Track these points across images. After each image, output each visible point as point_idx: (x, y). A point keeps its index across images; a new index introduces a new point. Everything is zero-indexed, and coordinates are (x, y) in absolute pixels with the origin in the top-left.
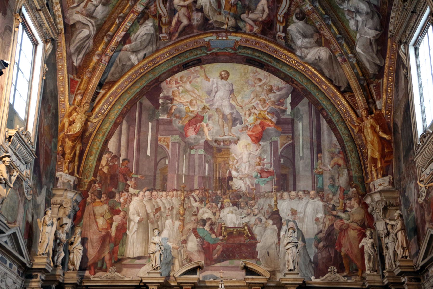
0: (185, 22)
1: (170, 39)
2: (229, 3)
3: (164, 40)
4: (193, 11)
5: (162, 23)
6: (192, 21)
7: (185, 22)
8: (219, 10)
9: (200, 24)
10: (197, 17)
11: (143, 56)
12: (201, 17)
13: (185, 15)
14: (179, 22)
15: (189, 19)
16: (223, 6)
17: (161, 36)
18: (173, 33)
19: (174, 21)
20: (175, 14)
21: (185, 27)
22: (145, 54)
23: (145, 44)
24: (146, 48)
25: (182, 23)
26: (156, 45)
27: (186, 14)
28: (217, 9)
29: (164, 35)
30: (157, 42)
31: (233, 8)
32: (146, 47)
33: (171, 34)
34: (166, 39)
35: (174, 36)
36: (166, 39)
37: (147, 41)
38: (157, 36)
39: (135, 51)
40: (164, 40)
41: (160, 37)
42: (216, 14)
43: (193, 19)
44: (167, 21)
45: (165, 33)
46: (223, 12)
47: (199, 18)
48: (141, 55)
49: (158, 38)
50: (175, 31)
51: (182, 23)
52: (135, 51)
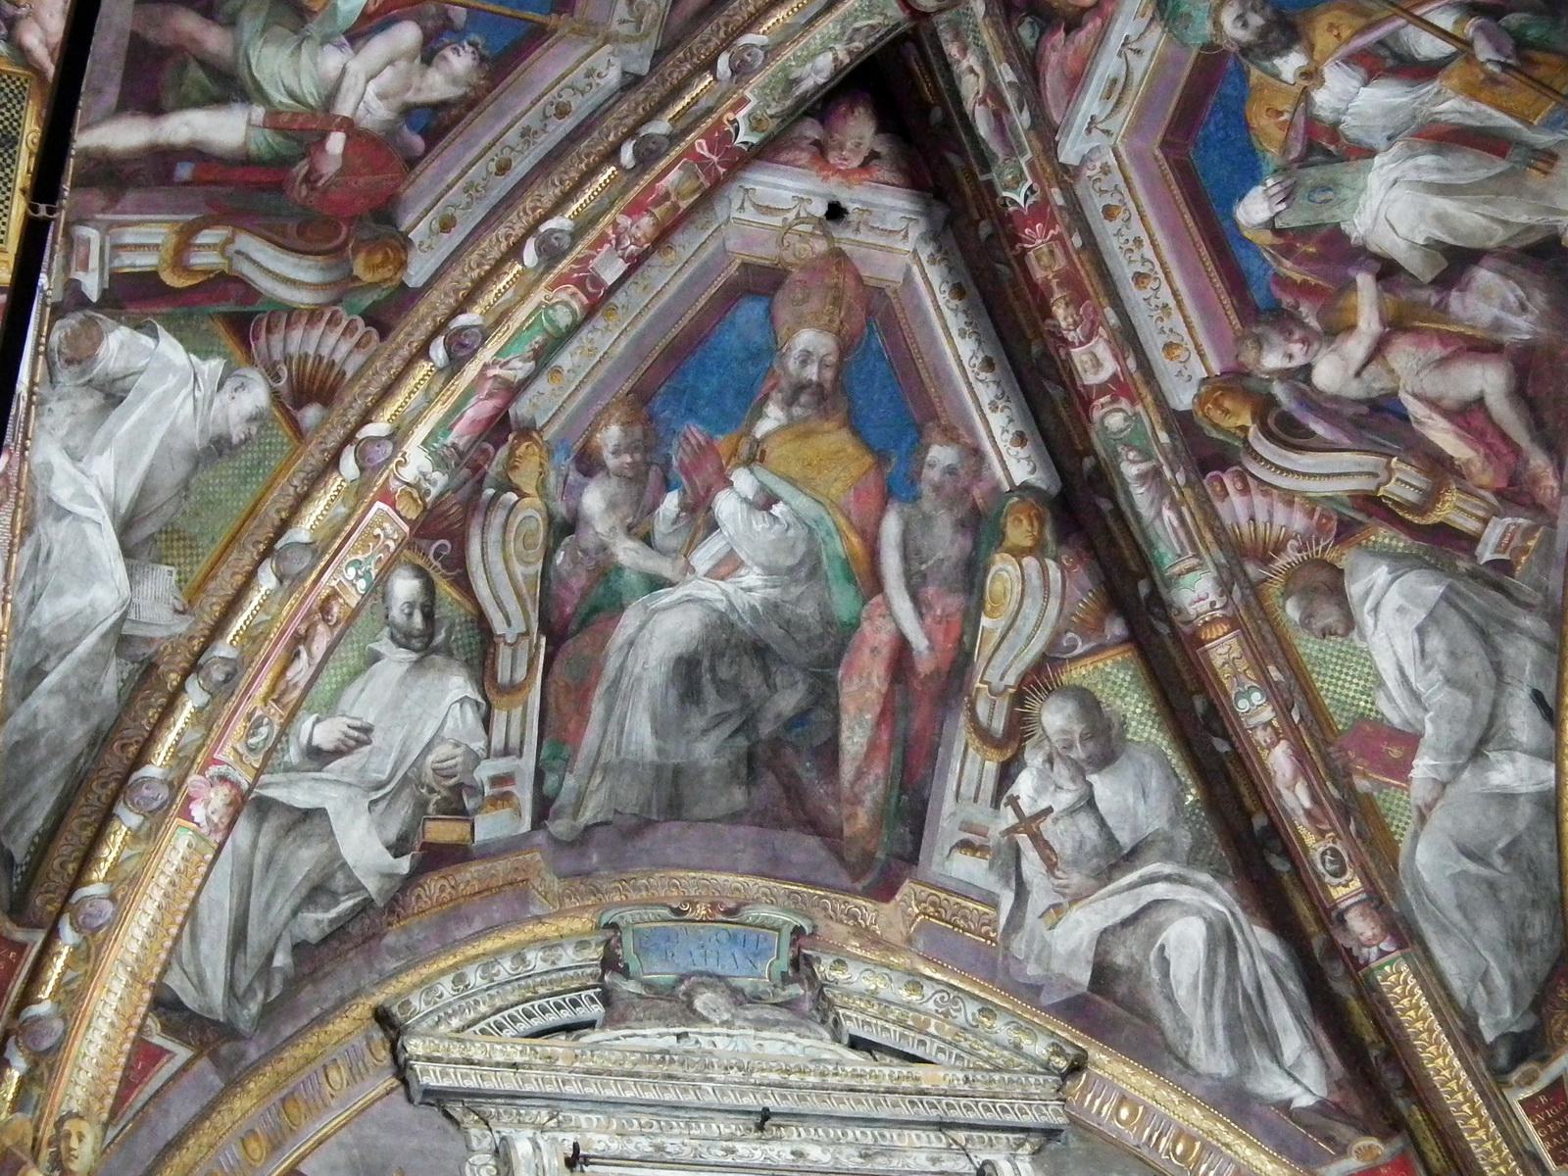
0: (1488, 380)
1: (1540, 510)
2: (1492, 80)
3: (1525, 551)
4: (1442, 308)
5: (1413, 508)
6: (1507, 338)
7: (1488, 380)
8: (1515, 155)
9: (1550, 303)
10: (1491, 300)
11: (1538, 716)
12: (1505, 275)
13: (1442, 363)
14: (1468, 415)
15: (1480, 347)
16: (1501, 120)
17: (1486, 553)
18: (1513, 480)
19: (1443, 436)
20: (1404, 417)
21: (1522, 392)
22: (1538, 697)
23: (1475, 665)
24: (1509, 671)
25: (1480, 401)
26: (1528, 607)
27: (1437, 351)
28: (1501, 166)
29: (1493, 533)
30: (1509, 595)
31: (1540, 72)
32: (1498, 669)
33: (1515, 494)
34: (1528, 533)
35: (1535, 481)
36: (1528, 533)
37: (1470, 643)
38: (1474, 575)
39: (1483, 741)
40: (1525, 551)
41: (1491, 563)
42: (1535, 180)
43: (1498, 325)
44: (1419, 481)
45: (1485, 522)
46: (1544, 139)
47: (1511, 292)
48: (1522, 721)
49: (1490, 573)
50: (1510, 459)
51: (1480, 401)
52: (1483, 741)
